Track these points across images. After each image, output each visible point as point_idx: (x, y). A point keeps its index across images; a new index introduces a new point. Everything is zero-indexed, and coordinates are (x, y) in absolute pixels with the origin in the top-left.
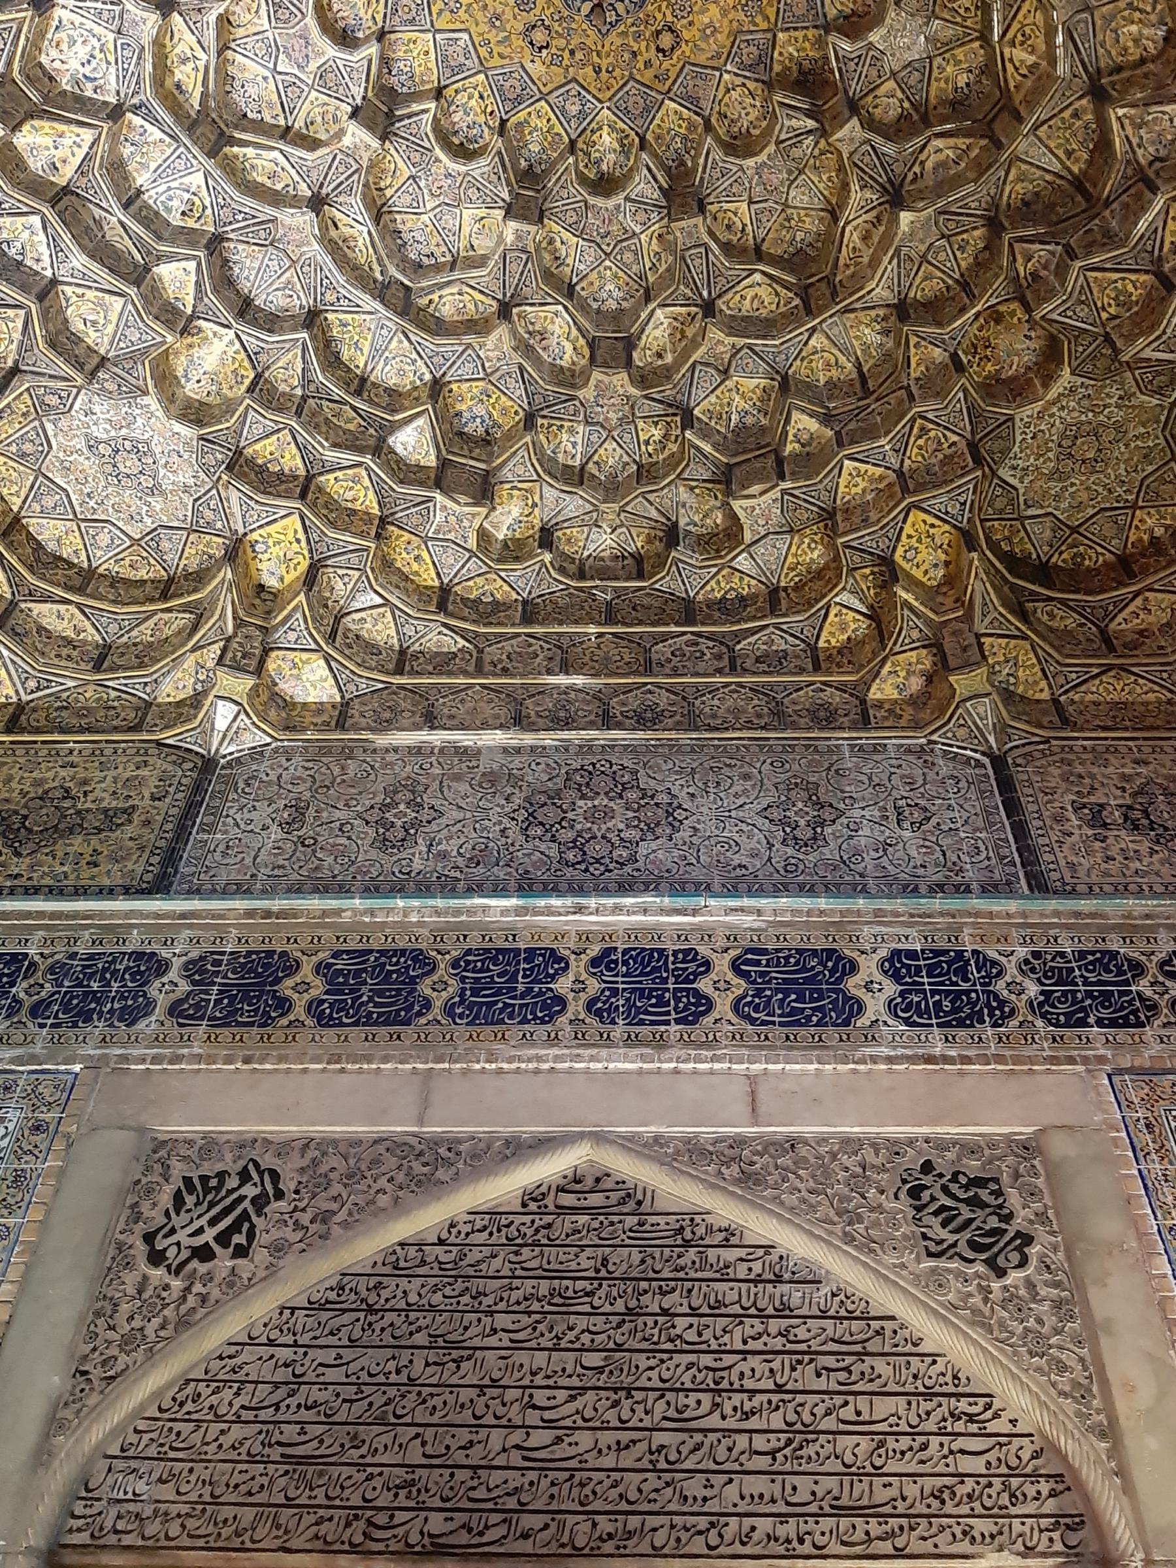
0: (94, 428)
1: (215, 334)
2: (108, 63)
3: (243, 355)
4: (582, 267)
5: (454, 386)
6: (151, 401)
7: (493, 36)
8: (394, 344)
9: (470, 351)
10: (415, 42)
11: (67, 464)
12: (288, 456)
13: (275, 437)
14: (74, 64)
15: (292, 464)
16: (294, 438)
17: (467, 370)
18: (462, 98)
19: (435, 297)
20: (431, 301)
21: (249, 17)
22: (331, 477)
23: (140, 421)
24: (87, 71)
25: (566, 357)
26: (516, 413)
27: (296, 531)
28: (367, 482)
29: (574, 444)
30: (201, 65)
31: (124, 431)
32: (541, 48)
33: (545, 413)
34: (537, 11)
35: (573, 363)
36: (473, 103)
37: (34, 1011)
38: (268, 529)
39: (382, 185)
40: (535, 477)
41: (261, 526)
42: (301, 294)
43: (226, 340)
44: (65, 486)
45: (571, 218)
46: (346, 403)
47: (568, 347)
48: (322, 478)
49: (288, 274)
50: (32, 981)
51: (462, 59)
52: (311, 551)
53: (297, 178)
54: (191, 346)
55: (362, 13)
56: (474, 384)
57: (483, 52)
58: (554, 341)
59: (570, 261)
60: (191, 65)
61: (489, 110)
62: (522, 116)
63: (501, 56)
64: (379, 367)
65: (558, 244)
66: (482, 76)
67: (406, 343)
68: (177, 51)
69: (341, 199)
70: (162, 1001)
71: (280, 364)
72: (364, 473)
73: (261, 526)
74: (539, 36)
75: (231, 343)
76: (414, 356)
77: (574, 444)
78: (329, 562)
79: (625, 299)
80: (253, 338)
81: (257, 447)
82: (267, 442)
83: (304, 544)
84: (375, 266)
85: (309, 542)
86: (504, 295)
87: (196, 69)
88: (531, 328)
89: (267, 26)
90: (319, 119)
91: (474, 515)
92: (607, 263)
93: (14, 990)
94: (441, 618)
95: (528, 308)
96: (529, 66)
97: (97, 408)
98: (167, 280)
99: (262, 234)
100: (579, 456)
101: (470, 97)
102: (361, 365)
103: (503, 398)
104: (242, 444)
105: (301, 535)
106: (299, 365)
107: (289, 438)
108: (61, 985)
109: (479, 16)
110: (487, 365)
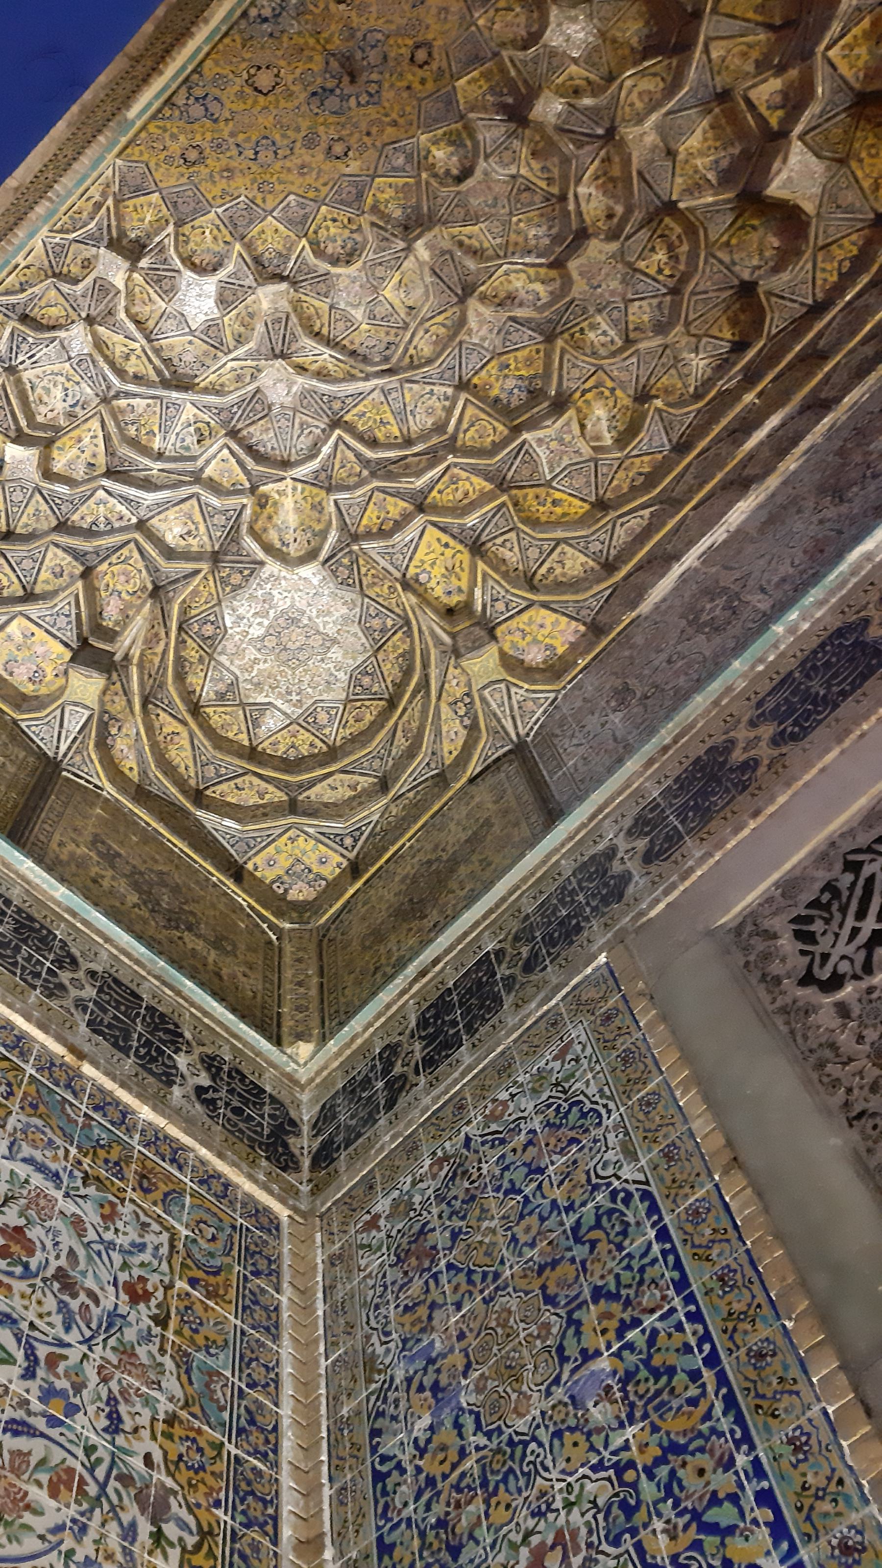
0: (251, 631)
1: (278, 492)
2: (78, 383)
3: (308, 487)
4: (499, 241)
5: (475, 380)
6: (272, 567)
7: (309, 179)
8: (408, 396)
9: (464, 346)
10: (263, 232)
11: (255, 680)
12: (390, 508)
13: (371, 504)
14: (60, 406)
15: (399, 509)
16: (384, 492)
17: (474, 362)
18: (322, 233)
19: (412, 351)
20: (411, 357)
21: (148, 308)
22: (434, 493)
23: (275, 592)
24: (70, 401)
25: (542, 294)
26: (538, 351)
27: (439, 540)
28: (464, 475)
29: (604, 333)
30: (139, 352)
31: (272, 612)
32: (346, 154)
33: (559, 330)
34: (324, 137)
35: (551, 293)
36: (333, 231)
37: (528, 968)
38: (418, 556)
39: (316, 329)
40: (593, 369)
41: (411, 559)
42: (316, 423)
43: (289, 491)
44: (267, 700)
45: (460, 213)
46: (406, 457)
47: (538, 287)
48: (429, 500)
49: (297, 421)
50: (508, 959)
51: (302, 212)
52: (461, 542)
53: (254, 363)
54: (270, 518)
55: (217, 249)
56: (489, 367)
57: (311, 195)
58: (522, 294)
59: (486, 245)
60: (133, 358)
61: (346, 221)
62: (370, 201)
63: (325, 184)
64: (411, 422)
65: (467, 241)
66: (324, 208)
67: (415, 387)
68: (118, 354)
69: (293, 349)
70: (633, 866)
71: (337, 467)
72: (456, 471)
73: (411, 559)
74: (338, 149)
75: (295, 489)
76: (428, 388)
77: (604, 333)
78: (483, 538)
79: (550, 228)
80: (304, 471)
81: (365, 522)
82: (368, 513)
83: (452, 543)
84: (353, 371)
85: (454, 537)
86: (456, 294)
87: (139, 357)
88: (497, 300)
89: (164, 305)
90: (242, 329)
91: (567, 424)
92: (515, 219)
93: (498, 976)
94: (613, 514)
95: (482, 288)
96: (348, 171)
97: (241, 611)
98: (216, 478)
99: (258, 407)
100: (616, 339)
101: (328, 229)
102: (398, 434)
103: (519, 354)
104: (353, 530)
105: (445, 538)
106: (350, 455)
107: (382, 496)
108: (534, 938)
109: (291, 177)
110: (486, 345)
